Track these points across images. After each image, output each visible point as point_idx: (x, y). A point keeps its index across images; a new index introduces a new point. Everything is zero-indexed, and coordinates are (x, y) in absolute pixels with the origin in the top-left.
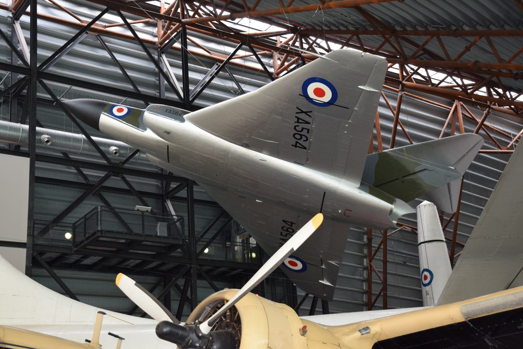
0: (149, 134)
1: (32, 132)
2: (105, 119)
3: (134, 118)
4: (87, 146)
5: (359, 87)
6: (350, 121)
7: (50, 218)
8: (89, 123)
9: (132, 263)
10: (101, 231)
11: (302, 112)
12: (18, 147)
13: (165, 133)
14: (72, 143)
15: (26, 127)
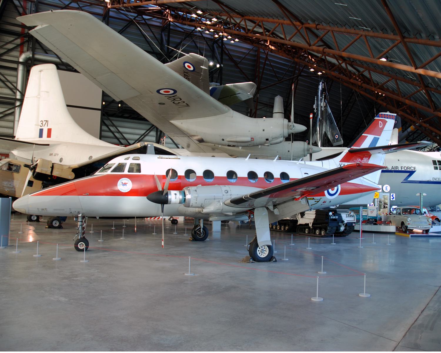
5: (201, 67)
6: (201, 77)
11: (185, 72)
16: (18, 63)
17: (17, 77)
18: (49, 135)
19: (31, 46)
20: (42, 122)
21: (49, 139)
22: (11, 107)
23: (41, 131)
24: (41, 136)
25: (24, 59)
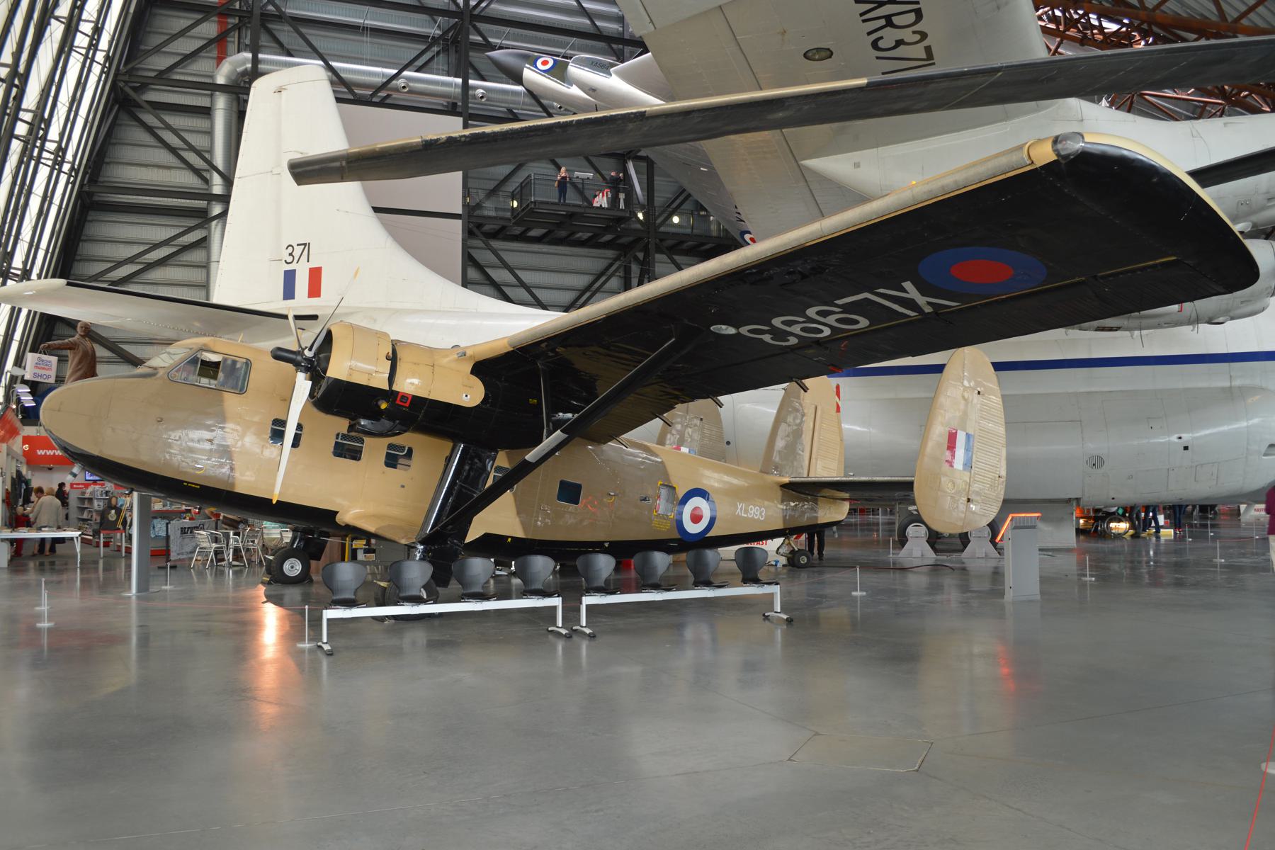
0: (575, 91)
1: (465, 86)
2: (528, 74)
3: (558, 72)
4: (528, 100)
7: (492, 185)
8: (518, 79)
9: (585, 236)
10: (535, 202)
12: (455, 105)
13: (591, 90)
14: (510, 98)
15: (459, 81)
16: (214, 88)
17: (210, 133)
18: (314, 291)
19: (247, 41)
20: (290, 249)
21: (314, 301)
22: (191, 222)
23: (290, 277)
24: (289, 293)
25: (228, 77)
